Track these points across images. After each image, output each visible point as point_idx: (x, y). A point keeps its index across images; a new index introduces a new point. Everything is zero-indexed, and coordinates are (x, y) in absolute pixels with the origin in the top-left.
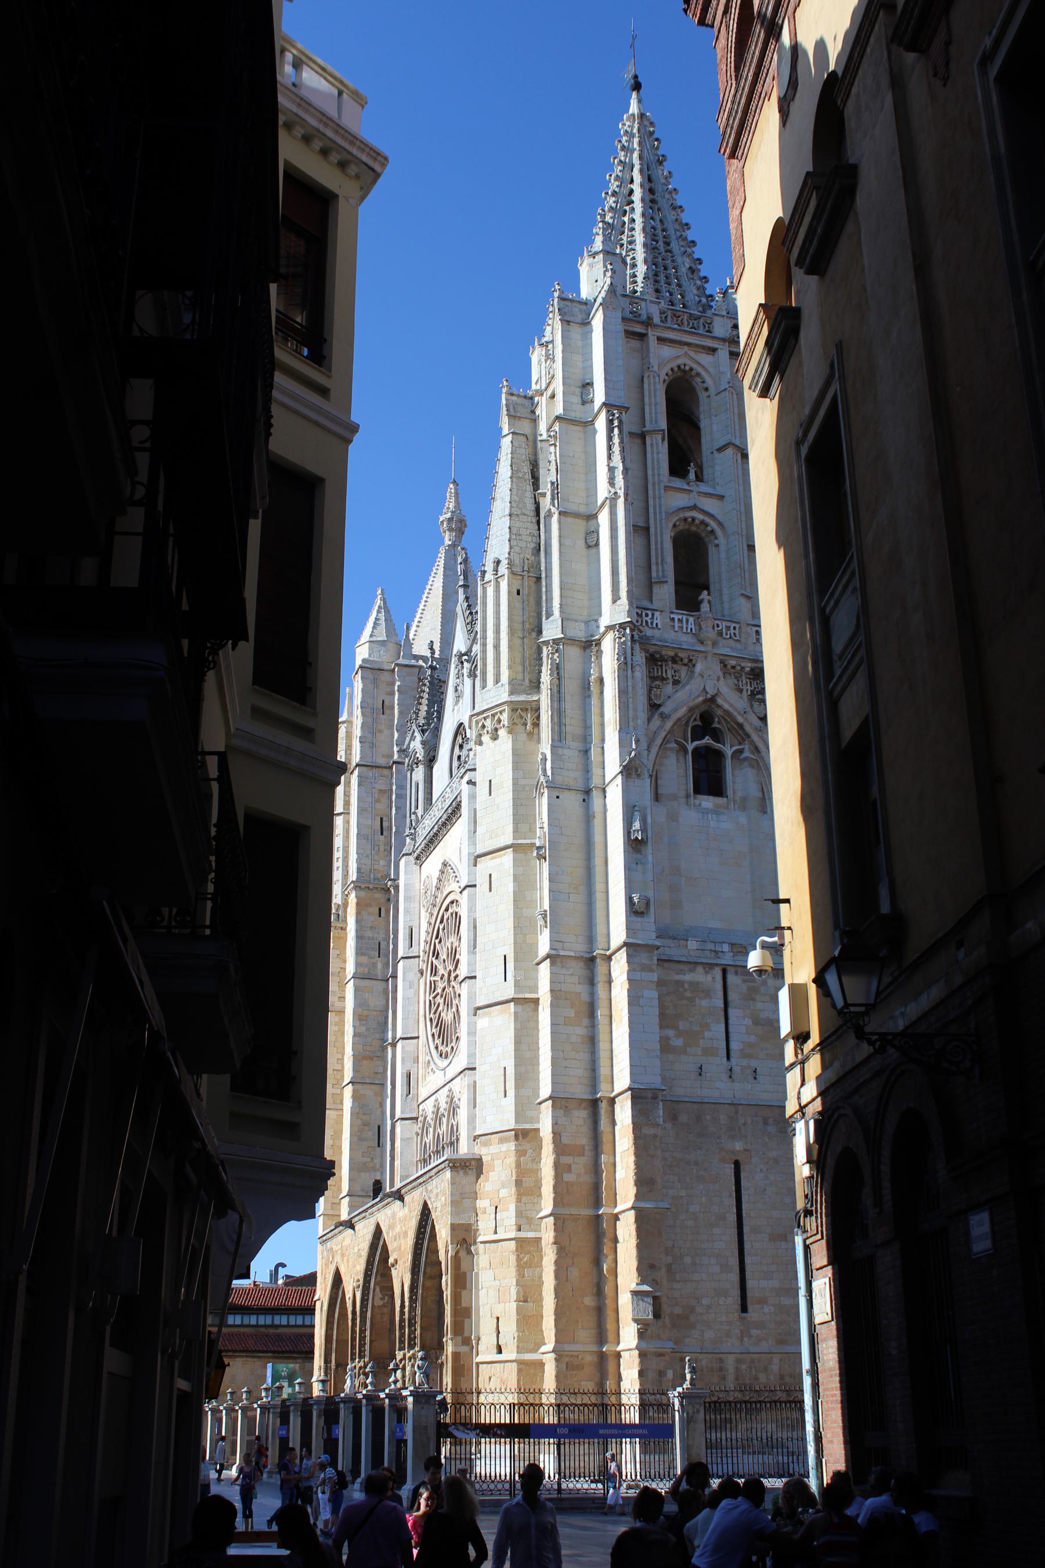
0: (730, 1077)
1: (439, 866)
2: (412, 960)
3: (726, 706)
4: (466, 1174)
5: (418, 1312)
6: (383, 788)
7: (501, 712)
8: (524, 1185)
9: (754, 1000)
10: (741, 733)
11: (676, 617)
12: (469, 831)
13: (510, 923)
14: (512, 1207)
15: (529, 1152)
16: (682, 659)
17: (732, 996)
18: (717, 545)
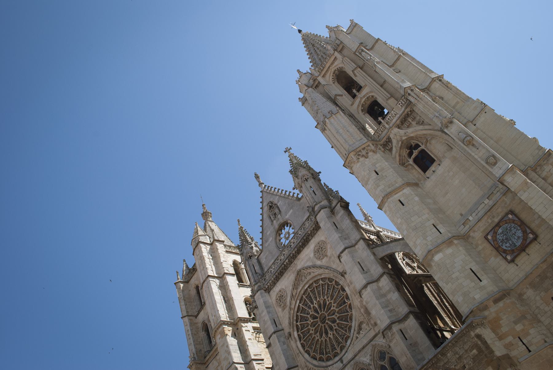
2: (280, 332)
14: (532, 331)
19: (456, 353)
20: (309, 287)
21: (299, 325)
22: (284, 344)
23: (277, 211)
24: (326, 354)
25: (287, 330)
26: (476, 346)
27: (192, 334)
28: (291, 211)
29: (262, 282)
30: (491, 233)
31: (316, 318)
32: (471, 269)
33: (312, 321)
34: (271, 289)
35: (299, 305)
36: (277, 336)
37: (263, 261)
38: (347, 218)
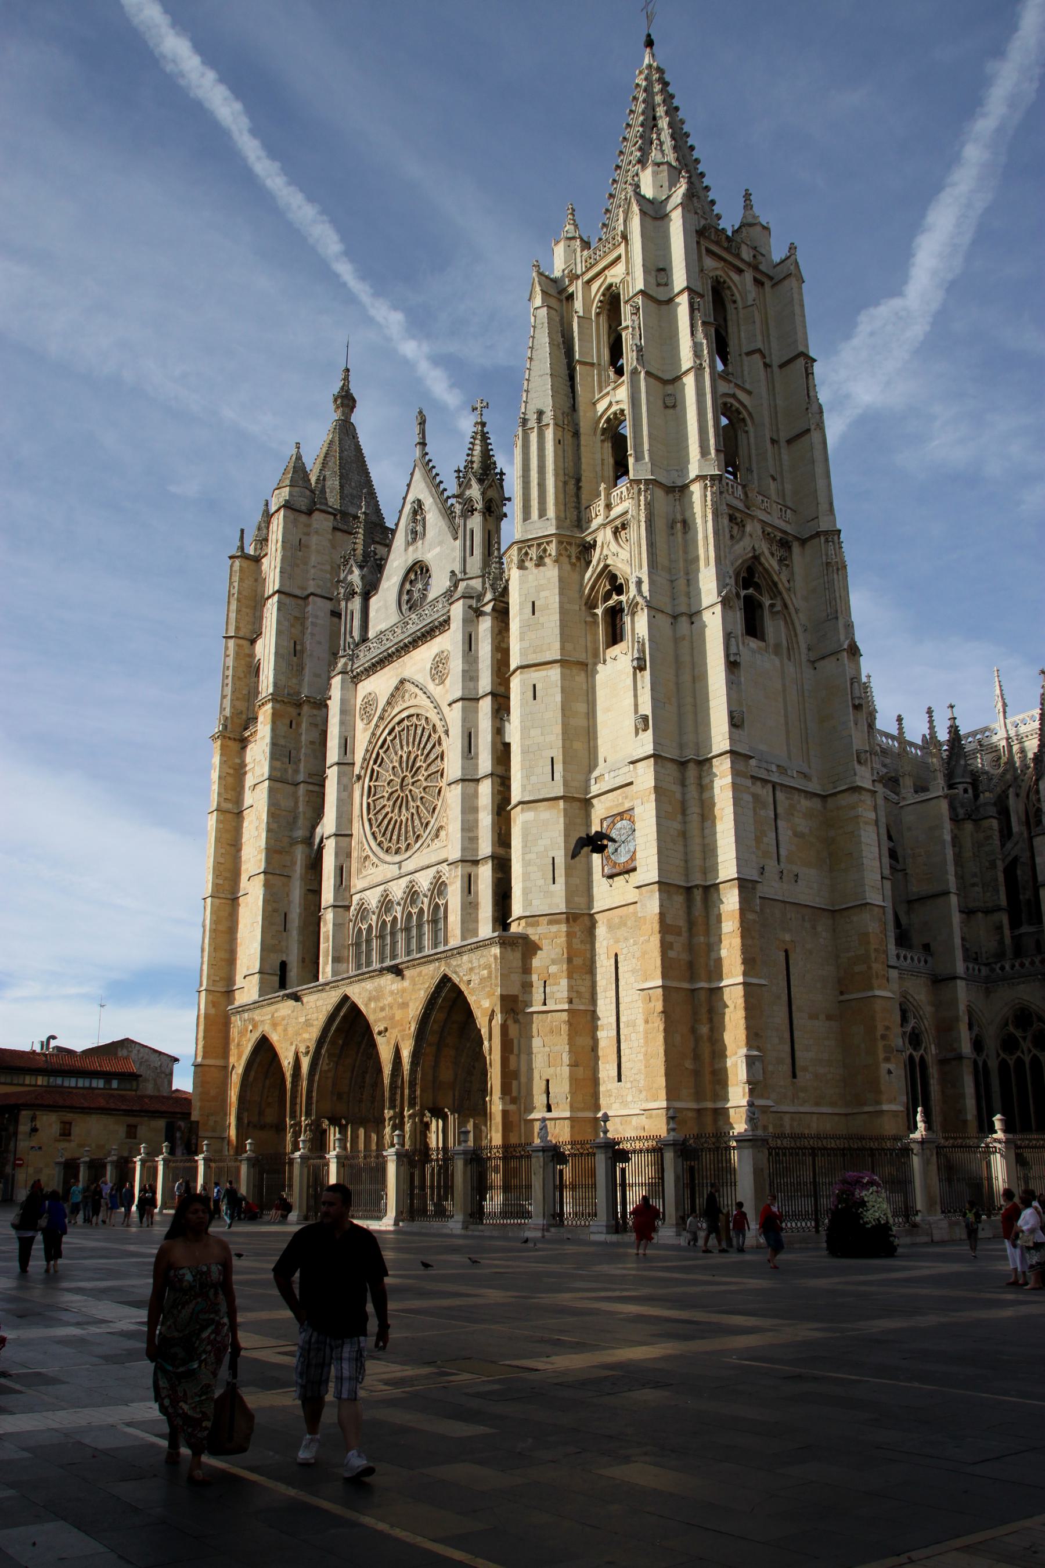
0: (781, 878)
1: (395, 682)
3: (767, 565)
4: (513, 950)
5: (419, 1076)
6: (298, 615)
7: (548, 543)
8: (575, 962)
9: (793, 815)
10: (774, 590)
11: (730, 483)
12: (463, 651)
13: (558, 729)
14: (564, 982)
15: (578, 936)
16: (736, 519)
17: (780, 810)
18: (747, 432)
19: (471, 962)
20: (408, 717)
21: (375, 774)
22: (344, 791)
23: (419, 528)
24: (390, 841)
25: (357, 770)
26: (487, 967)
27: (233, 676)
28: (438, 549)
29: (352, 660)
30: (609, 820)
31: (398, 777)
32: (553, 858)
33: (392, 777)
34: (361, 681)
35: (385, 740)
36: (339, 772)
37: (372, 614)
38: (490, 640)
